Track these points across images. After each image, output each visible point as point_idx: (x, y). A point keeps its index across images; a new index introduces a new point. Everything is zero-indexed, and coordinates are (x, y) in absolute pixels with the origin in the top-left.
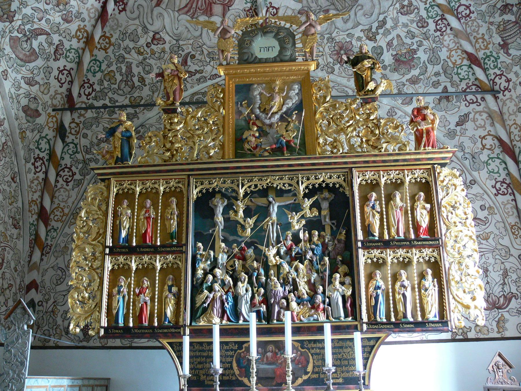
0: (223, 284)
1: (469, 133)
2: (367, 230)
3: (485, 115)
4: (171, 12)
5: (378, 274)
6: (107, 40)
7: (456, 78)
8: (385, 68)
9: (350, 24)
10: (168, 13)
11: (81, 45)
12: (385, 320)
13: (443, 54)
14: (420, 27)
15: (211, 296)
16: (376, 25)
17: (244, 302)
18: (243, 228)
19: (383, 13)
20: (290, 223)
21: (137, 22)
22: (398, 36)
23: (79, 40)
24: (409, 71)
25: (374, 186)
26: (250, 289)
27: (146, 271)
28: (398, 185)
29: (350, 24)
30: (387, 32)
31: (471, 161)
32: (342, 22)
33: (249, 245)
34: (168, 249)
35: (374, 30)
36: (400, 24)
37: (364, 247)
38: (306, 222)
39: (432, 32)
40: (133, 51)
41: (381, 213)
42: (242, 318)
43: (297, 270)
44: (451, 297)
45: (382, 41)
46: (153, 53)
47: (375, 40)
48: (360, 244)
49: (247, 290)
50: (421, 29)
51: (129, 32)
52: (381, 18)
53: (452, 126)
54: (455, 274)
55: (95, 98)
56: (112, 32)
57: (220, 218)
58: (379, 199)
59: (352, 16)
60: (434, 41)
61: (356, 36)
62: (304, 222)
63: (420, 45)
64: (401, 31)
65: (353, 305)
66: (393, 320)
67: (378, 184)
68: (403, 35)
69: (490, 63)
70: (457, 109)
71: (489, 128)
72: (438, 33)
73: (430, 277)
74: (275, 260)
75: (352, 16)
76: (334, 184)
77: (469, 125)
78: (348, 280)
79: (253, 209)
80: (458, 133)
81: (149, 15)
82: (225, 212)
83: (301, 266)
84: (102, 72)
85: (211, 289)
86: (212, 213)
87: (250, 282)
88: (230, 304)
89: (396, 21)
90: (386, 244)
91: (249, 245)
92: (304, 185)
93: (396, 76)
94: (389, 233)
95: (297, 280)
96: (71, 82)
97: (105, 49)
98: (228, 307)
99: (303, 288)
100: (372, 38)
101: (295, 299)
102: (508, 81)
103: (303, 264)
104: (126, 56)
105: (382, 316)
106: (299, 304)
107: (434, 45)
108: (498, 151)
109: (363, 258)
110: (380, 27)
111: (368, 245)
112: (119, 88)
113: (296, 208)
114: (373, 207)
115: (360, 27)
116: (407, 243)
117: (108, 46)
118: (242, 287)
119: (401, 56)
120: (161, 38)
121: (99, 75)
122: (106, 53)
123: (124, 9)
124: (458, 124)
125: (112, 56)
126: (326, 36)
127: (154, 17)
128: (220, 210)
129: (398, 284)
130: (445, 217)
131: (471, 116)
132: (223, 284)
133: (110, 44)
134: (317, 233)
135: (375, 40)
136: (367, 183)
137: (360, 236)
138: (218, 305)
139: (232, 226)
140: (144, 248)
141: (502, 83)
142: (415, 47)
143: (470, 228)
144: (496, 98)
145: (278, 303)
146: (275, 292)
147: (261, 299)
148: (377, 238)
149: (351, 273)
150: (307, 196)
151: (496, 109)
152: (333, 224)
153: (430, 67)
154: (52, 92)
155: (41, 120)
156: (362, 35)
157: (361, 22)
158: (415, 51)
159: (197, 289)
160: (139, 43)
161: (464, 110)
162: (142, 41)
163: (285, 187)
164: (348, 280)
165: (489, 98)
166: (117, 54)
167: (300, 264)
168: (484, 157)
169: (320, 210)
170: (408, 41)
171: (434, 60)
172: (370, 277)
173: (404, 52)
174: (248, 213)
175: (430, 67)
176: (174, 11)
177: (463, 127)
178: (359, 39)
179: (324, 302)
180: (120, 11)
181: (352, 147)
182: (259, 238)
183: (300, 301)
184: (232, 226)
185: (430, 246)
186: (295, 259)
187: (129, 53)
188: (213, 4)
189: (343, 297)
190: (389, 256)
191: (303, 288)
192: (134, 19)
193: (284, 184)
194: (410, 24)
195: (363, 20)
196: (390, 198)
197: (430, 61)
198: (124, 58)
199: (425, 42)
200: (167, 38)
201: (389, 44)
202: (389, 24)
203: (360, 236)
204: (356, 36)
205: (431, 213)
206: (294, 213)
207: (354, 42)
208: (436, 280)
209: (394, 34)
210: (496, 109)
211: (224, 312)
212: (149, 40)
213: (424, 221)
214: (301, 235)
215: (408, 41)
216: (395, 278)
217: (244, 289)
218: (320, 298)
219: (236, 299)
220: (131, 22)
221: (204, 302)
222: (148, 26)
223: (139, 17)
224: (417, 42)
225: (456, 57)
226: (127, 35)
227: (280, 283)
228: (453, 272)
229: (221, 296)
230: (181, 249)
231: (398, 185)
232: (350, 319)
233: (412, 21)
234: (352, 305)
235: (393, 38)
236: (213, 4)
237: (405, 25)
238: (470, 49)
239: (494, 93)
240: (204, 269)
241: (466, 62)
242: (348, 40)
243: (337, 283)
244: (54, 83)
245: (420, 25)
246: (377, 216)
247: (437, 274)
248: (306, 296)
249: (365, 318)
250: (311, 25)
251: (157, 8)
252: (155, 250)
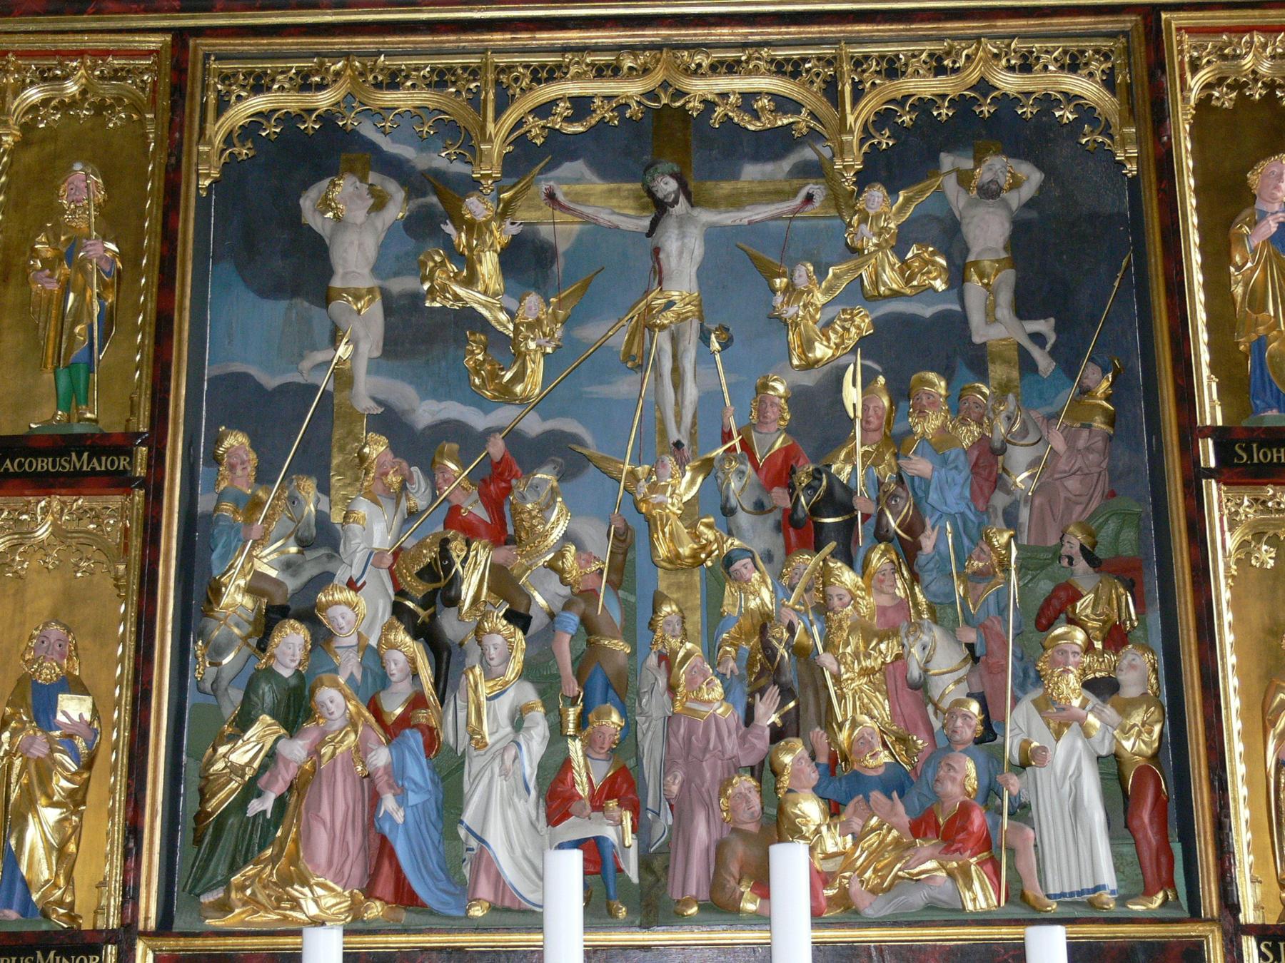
34: (43, 464)
38: (875, 323)
48: (1208, 454)
49: (518, 720)
62: (863, 323)
74: (696, 537)
76: (1048, 102)
78: (1138, 669)
79: (562, 247)
85: (296, 708)
87: (538, 671)
88: (413, 799)
92: (870, 105)
95: (827, 660)
98: (399, 817)
106: (834, 810)
136: (1243, 100)
146: (690, 732)
147: (601, 771)
152: (1038, 338)
163: (756, 115)
167: (836, 565)
183: (841, 786)
191: (863, 714)
193: (748, 98)
214: (852, 395)
221: (251, 790)
227: (722, 677)
229: (361, 751)
230: (123, 463)
240: (257, 587)
243: (1070, 688)
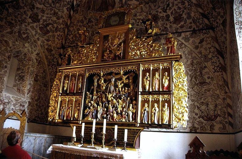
0: (94, 107)
1: (204, 47)
2: (144, 87)
3: (210, 39)
4: (94, 11)
5: (146, 105)
6: (73, 24)
7: (198, 24)
8: (171, 23)
9: (157, 7)
10: (93, 12)
11: (64, 26)
12: (146, 123)
13: (192, 14)
14: (182, 5)
15: (89, 111)
16: (166, 6)
17: (99, 113)
18: (103, 87)
19: (168, 1)
20: (118, 85)
21: (82, 16)
22: (175, 9)
23: (63, 25)
24: (180, 23)
25: (148, 70)
26: (102, 109)
29: (157, 7)
30: (170, 9)
31: (204, 58)
32: (154, 7)
33: (103, 92)
35: (165, 8)
36: (175, 4)
37: (141, 94)
39: (187, 6)
40: (82, 26)
41: (150, 81)
42: (98, 119)
43: (118, 102)
44: (173, 115)
45: (169, 12)
46: (89, 26)
47: (166, 12)
48: (140, 93)
49: (101, 109)
50: (183, 5)
51: (80, 20)
52: (167, 3)
53: (197, 44)
54: (176, 105)
55: (71, 44)
56: (74, 21)
57: (96, 84)
58: (149, 75)
59: (157, 4)
60: (188, 10)
61: (159, 11)
62: (123, 85)
63: (183, 12)
64: (175, 7)
65: (135, 116)
66: (150, 123)
67: (150, 69)
68: (176, 8)
69: (210, 16)
70: (199, 37)
71: (212, 44)
72: (190, 6)
73: (166, 107)
75: (157, 4)
77: (204, 43)
80: (200, 47)
81: (86, 13)
82: (98, 81)
83: (120, 101)
84: (73, 34)
85: (89, 108)
86: (93, 82)
89: (173, 3)
90: (149, 93)
91: (103, 92)
93: (175, 25)
94: (152, 89)
96: (62, 39)
97: (73, 27)
100: (165, 12)
101: (116, 113)
102: (217, 23)
103: (121, 100)
104: (80, 28)
105: (145, 121)
107: (189, 11)
108: (216, 53)
109: (140, 98)
110: (167, 7)
111: (143, 93)
112: (79, 40)
113: (120, 79)
114: (147, 78)
115: (160, 8)
116: (158, 93)
117: (73, 26)
119: (176, 17)
120: (91, 20)
121: (71, 36)
122: (73, 28)
123: (77, 13)
124: (199, 43)
125: (75, 29)
126: (148, 13)
127: (88, 14)
128: (96, 81)
129: (154, 109)
130: (175, 82)
131: (205, 39)
132: (94, 107)
133: (74, 25)
134: (127, 89)
135: (166, 12)
137: (141, 89)
138: (91, 113)
139: (99, 86)
140: (72, 94)
141: (215, 24)
142: (181, 13)
143: (185, 87)
144: (214, 31)
145: (110, 114)
148: (147, 91)
150: (125, 74)
151: (214, 35)
153: (188, 20)
154: (56, 43)
155: (53, 52)
156: (161, 11)
157: (160, 6)
158: (182, 15)
160: (84, 23)
161: (202, 37)
162: (85, 23)
164: (135, 107)
165: (211, 31)
166: (77, 28)
168: (210, 56)
169: (129, 80)
170: (178, 11)
171: (189, 17)
172: (143, 106)
173: (177, 15)
174: (105, 81)
175: (188, 20)
176: (95, 11)
177: (202, 44)
178: (160, 12)
179: (125, 114)
180: (76, 14)
181: (141, 55)
183: (117, 113)
185: (167, 94)
186: (118, 98)
187: (81, 27)
188: (108, 7)
189: (133, 113)
190: (151, 98)
191: (119, 109)
192: (81, 15)
194: (178, 4)
195: (161, 5)
196: (154, 75)
197: (188, 18)
198: (79, 29)
199: (185, 11)
200: (94, 21)
201: (172, 13)
202: (171, 5)
203: (141, 89)
204: (159, 11)
205: (169, 81)
206: (119, 81)
207: (159, 14)
208: (168, 108)
209: (173, 9)
210: (214, 35)
211: (93, 116)
212: (87, 22)
213: (166, 85)
215: (178, 11)
216: (153, 106)
217: (100, 108)
218: (124, 113)
219: (97, 111)
220: (80, 17)
222: (87, 17)
223: (83, 15)
224: (182, 11)
225: (197, 15)
226: (80, 21)
228: (176, 105)
232: (134, 121)
233: (179, 3)
235: (173, 10)
236: (108, 7)
237: (177, 5)
238: (201, 11)
239: (213, 28)
241: (201, 17)
242: (156, 13)
243: (131, 108)
244: (56, 40)
245: (182, 4)
246: (148, 82)
247: (169, 106)
248: (119, 112)
249: (139, 121)
250: (129, 10)
251: (89, 11)
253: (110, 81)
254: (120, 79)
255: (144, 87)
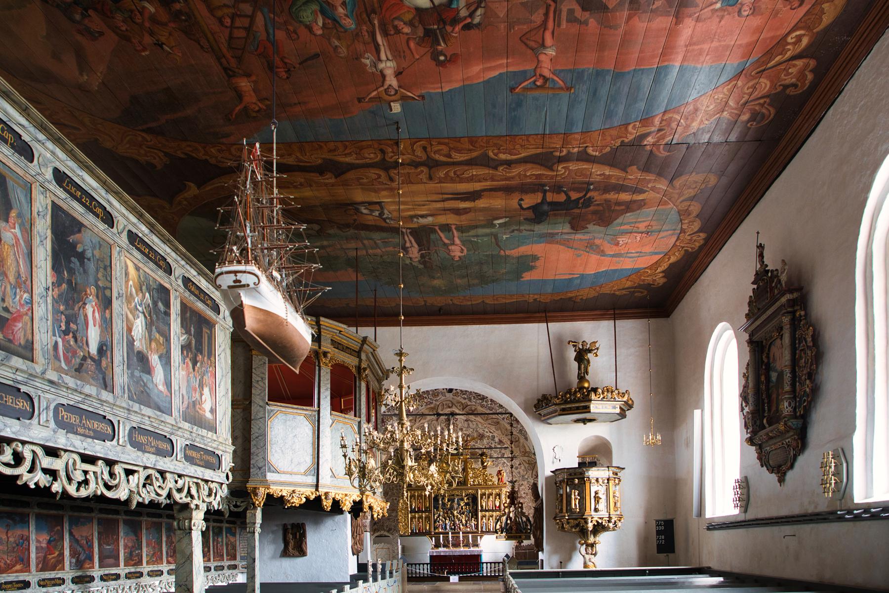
2: (482, 506)
25: (485, 494)
27: (421, 517)
28: (491, 494)
90: (486, 511)
99: (464, 522)
109: (480, 514)
113: (462, 500)
116: (493, 511)
118: (447, 522)
139: (444, 504)
149: (477, 518)
159: (435, 522)
174: (449, 501)
182: (452, 508)
184: (444, 504)
190: (487, 514)
191: (464, 522)
196: (489, 497)
213: (498, 505)
231: (491, 494)
234: (477, 526)
252: (423, 512)
253: (453, 501)
254: (462, 500)
255: (482, 506)
